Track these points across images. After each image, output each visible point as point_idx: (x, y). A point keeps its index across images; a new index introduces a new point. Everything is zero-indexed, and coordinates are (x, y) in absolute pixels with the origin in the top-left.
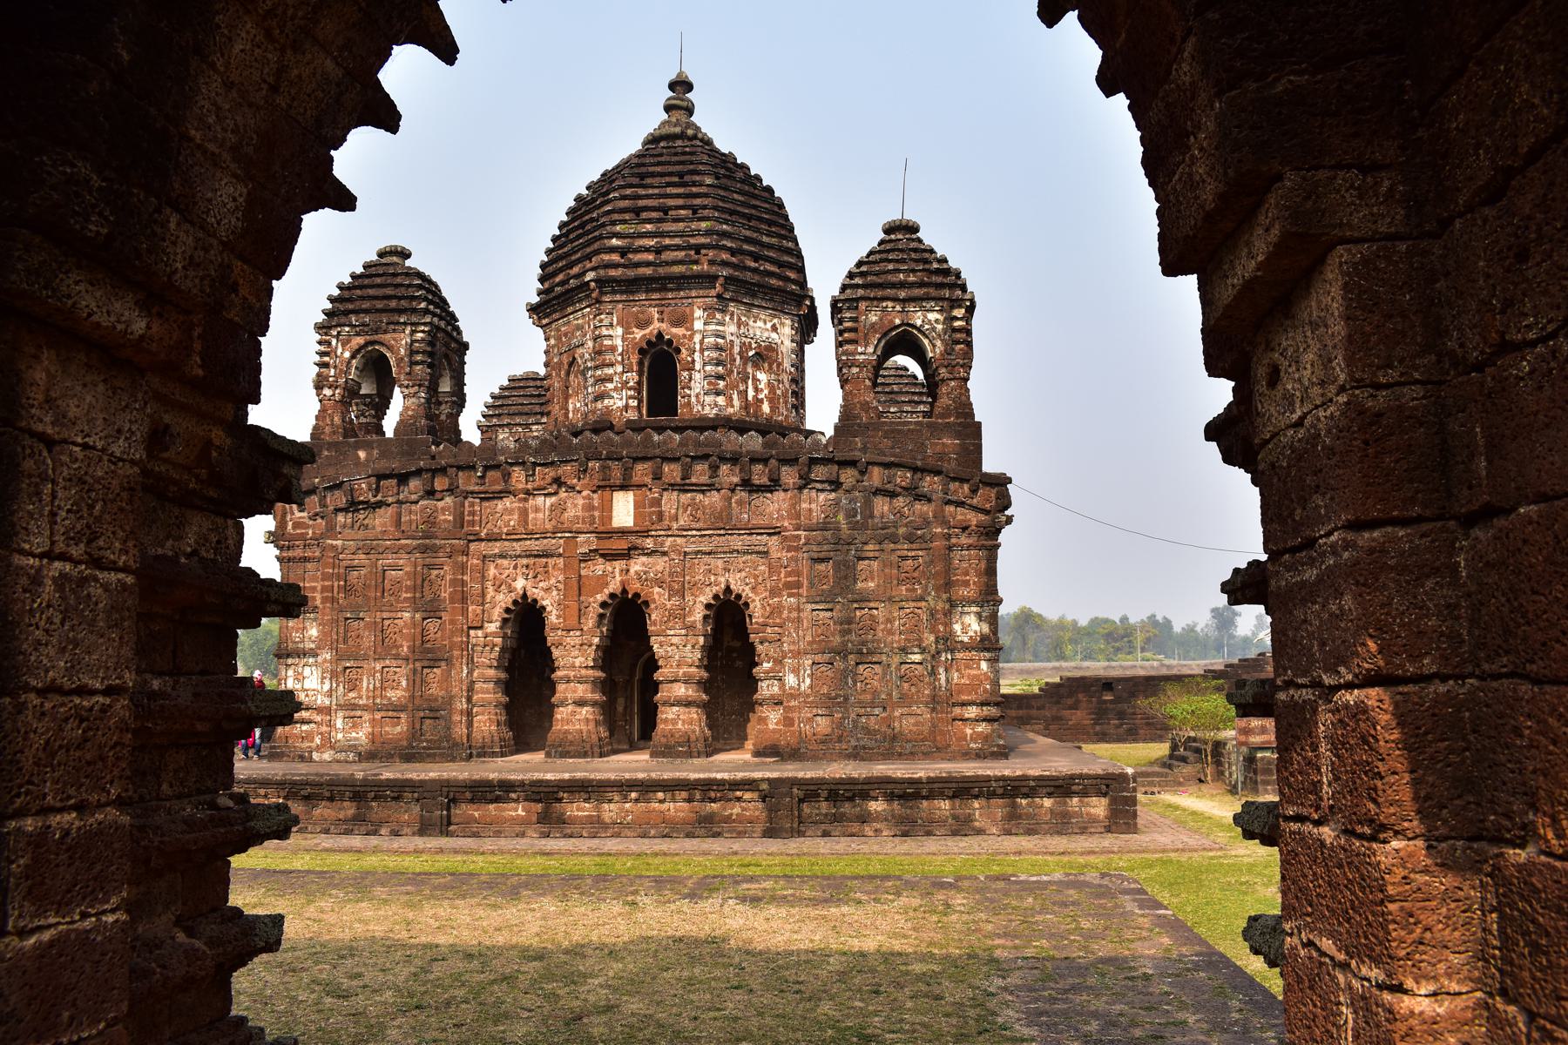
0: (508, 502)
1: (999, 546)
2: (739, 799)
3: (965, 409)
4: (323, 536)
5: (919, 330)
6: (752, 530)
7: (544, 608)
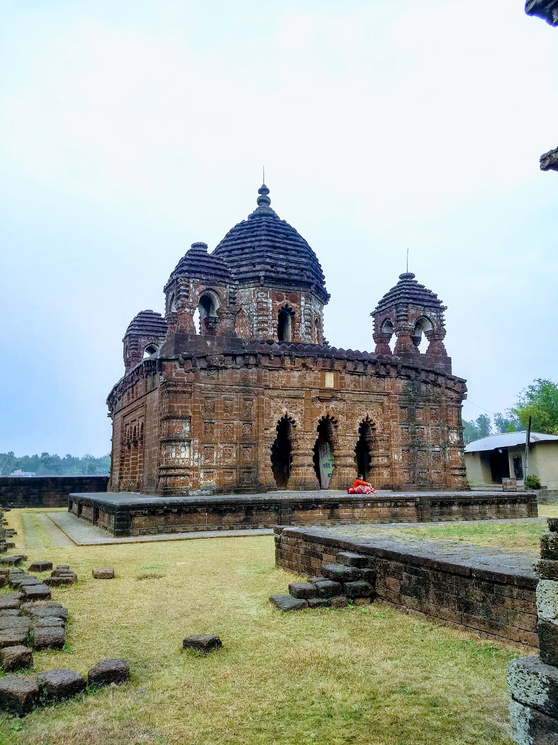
0: (281, 372)
1: (463, 406)
2: (407, 506)
3: (444, 352)
4: (194, 381)
5: (428, 319)
6: (379, 393)
7: (294, 422)
